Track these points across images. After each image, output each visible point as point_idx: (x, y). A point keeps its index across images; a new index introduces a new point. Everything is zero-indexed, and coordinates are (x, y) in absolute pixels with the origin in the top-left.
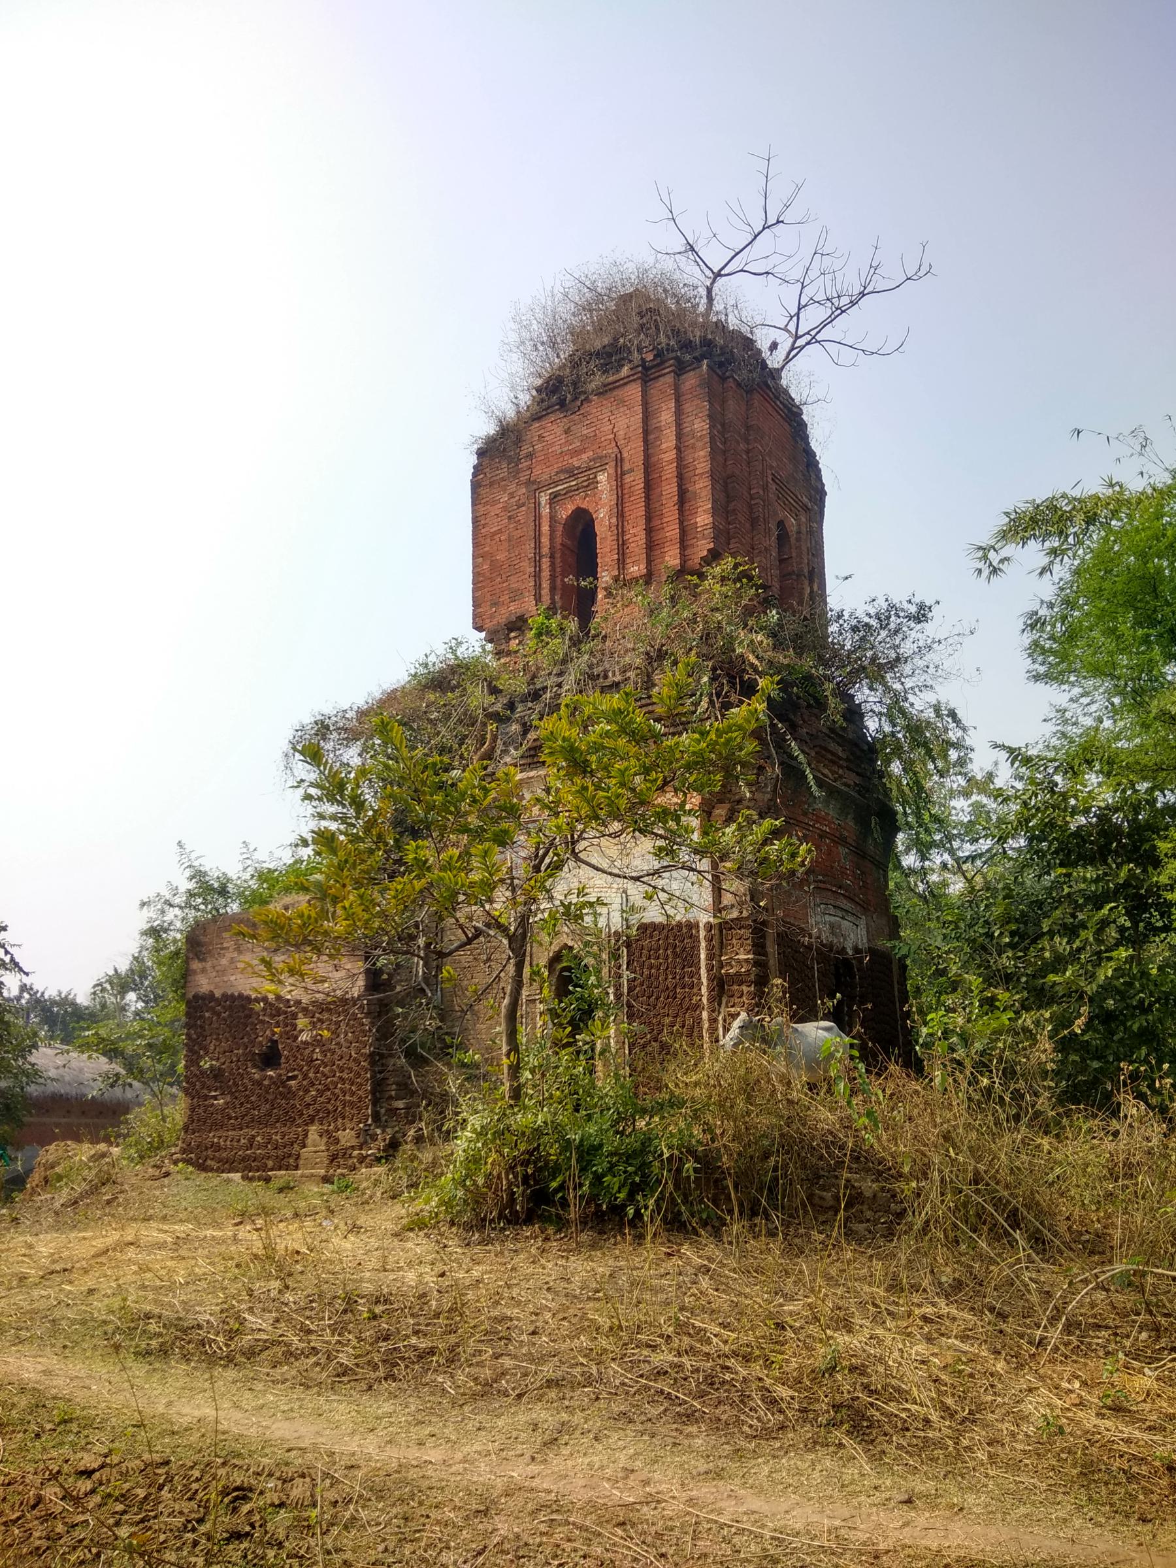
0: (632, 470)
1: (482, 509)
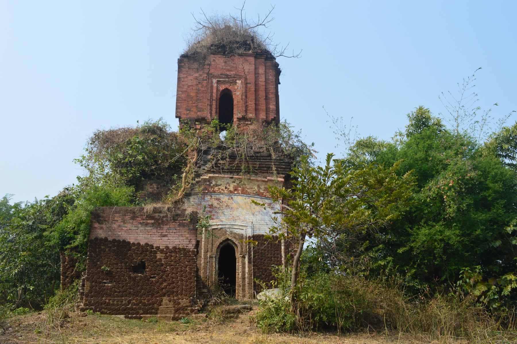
0: (250, 83)
1: (182, 75)
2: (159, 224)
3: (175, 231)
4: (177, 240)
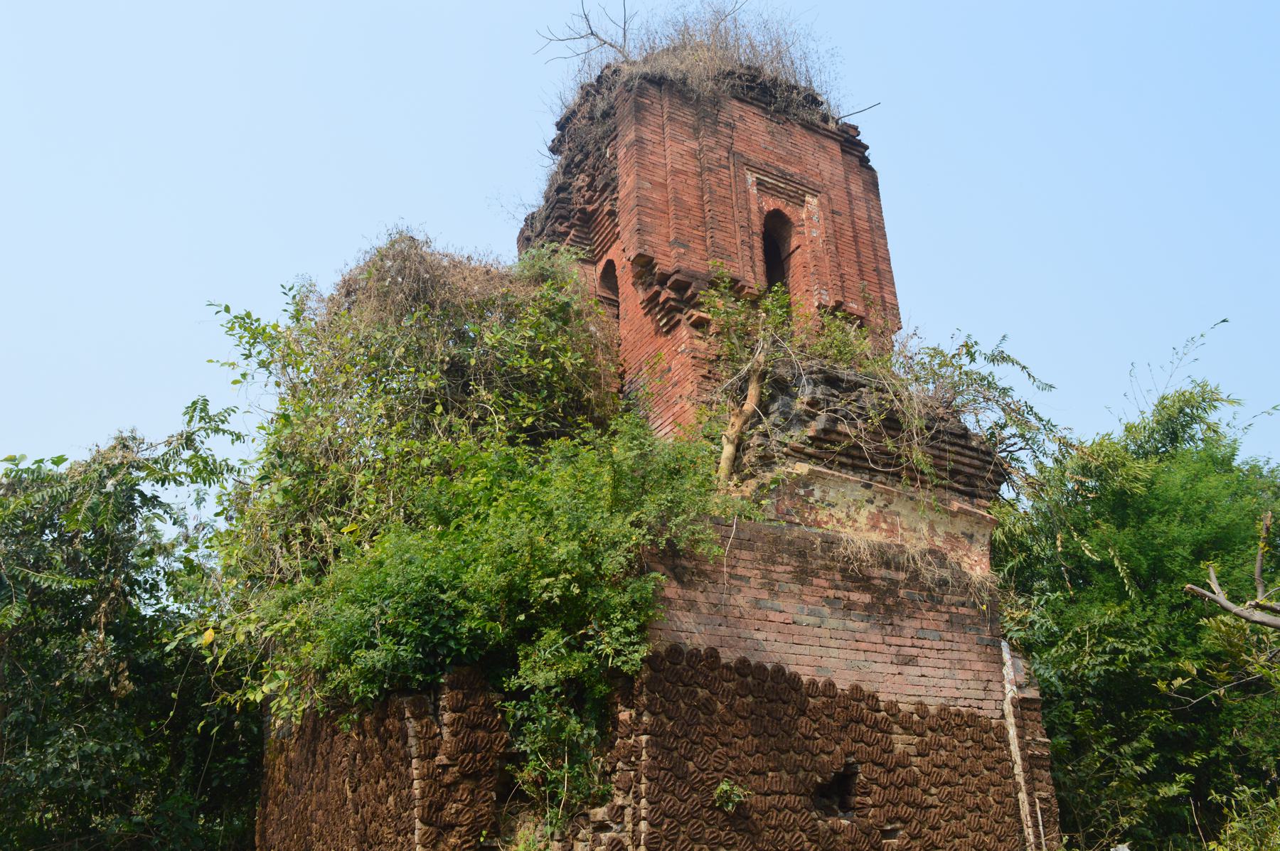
2: (889, 611)
3: (940, 645)
4: (949, 682)
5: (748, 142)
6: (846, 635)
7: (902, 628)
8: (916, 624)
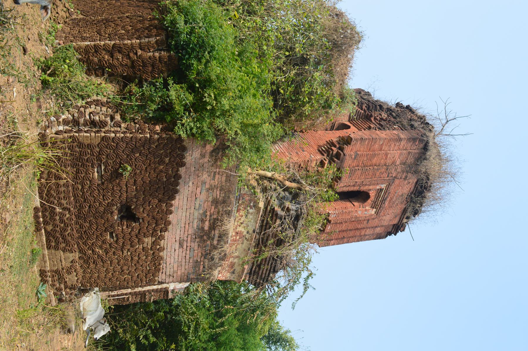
2: (201, 237)
3: (188, 257)
4: (172, 260)
5: (399, 185)
6: (191, 219)
7: (194, 242)
8: (196, 248)
